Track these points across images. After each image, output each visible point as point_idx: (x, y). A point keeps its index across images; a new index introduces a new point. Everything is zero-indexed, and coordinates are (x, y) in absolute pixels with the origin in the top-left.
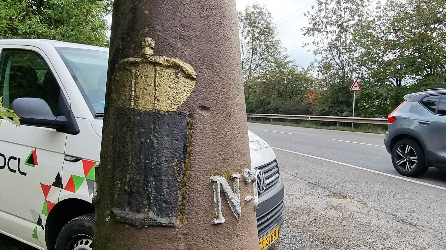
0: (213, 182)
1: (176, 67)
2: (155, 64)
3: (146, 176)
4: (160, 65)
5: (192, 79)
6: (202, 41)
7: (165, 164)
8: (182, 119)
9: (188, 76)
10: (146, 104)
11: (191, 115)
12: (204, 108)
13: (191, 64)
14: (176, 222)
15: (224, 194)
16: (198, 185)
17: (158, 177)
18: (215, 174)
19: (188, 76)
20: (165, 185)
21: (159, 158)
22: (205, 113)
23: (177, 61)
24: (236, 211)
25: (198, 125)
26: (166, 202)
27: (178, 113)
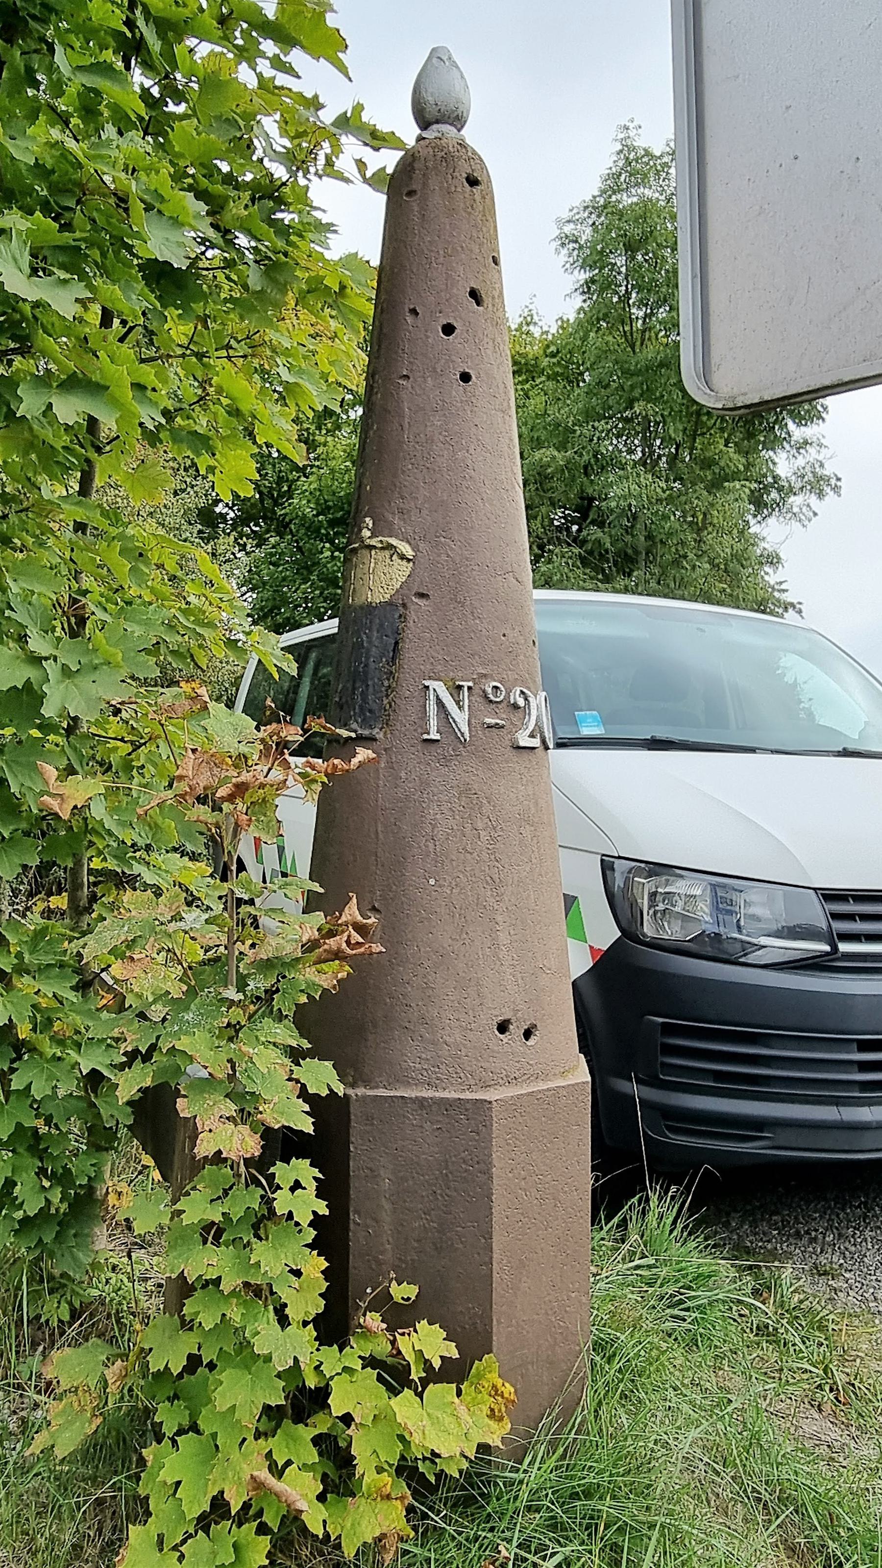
0: (427, 687)
1: (390, 547)
2: (371, 547)
3: (354, 682)
4: (375, 547)
5: (409, 560)
6: (425, 512)
7: (372, 666)
8: (395, 608)
9: (402, 557)
10: (359, 600)
11: (404, 605)
12: (422, 595)
13: (408, 542)
14: (380, 736)
15: (440, 703)
16: (407, 686)
17: (365, 681)
18: (430, 678)
19: (402, 557)
20: (371, 690)
21: (367, 658)
22: (421, 602)
23: (393, 541)
24: (462, 734)
25: (412, 616)
26: (370, 711)
27: (390, 604)
